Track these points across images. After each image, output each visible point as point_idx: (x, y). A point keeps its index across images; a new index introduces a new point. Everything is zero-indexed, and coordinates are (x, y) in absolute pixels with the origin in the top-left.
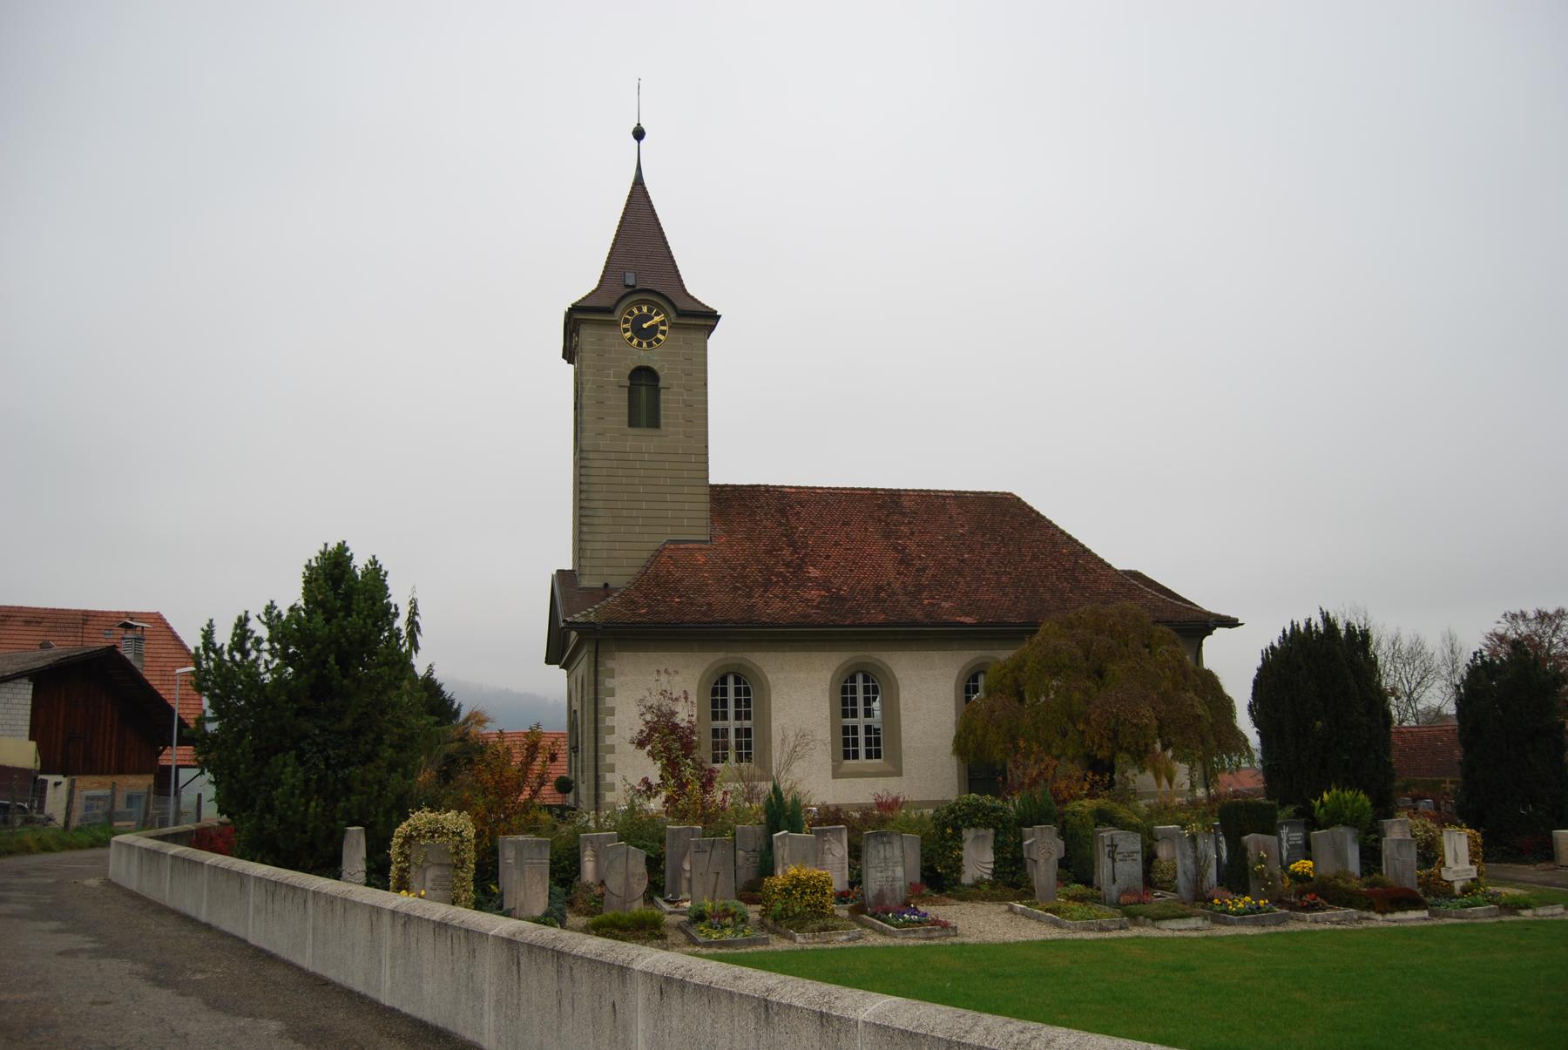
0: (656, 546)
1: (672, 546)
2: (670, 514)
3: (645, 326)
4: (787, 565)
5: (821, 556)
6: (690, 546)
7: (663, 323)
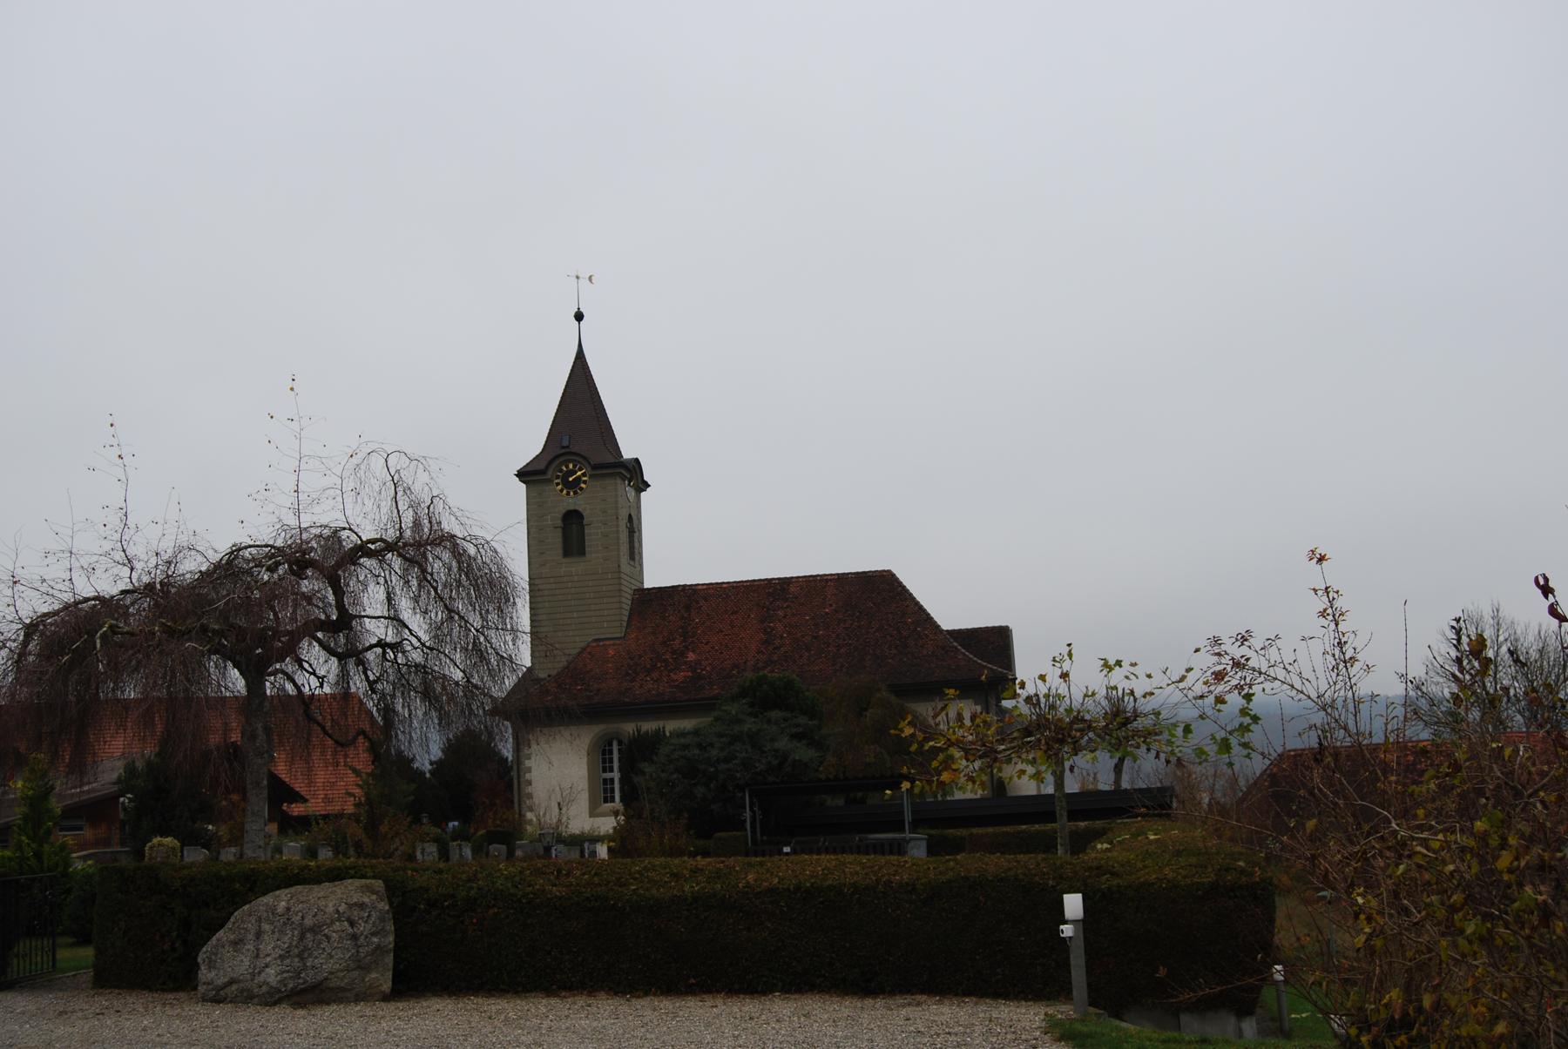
0: (583, 645)
1: (594, 644)
3: (571, 479)
5: (702, 642)
6: (607, 643)
7: (584, 475)
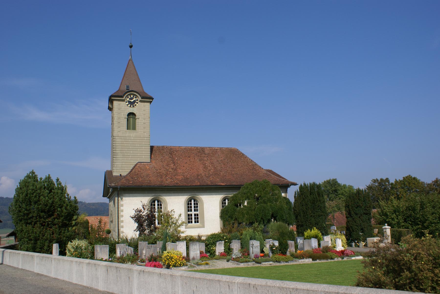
0: (135, 164)
1: (140, 164)
2: (139, 154)
4: (172, 169)
6: (145, 163)
